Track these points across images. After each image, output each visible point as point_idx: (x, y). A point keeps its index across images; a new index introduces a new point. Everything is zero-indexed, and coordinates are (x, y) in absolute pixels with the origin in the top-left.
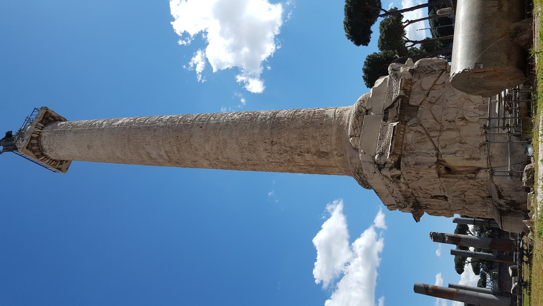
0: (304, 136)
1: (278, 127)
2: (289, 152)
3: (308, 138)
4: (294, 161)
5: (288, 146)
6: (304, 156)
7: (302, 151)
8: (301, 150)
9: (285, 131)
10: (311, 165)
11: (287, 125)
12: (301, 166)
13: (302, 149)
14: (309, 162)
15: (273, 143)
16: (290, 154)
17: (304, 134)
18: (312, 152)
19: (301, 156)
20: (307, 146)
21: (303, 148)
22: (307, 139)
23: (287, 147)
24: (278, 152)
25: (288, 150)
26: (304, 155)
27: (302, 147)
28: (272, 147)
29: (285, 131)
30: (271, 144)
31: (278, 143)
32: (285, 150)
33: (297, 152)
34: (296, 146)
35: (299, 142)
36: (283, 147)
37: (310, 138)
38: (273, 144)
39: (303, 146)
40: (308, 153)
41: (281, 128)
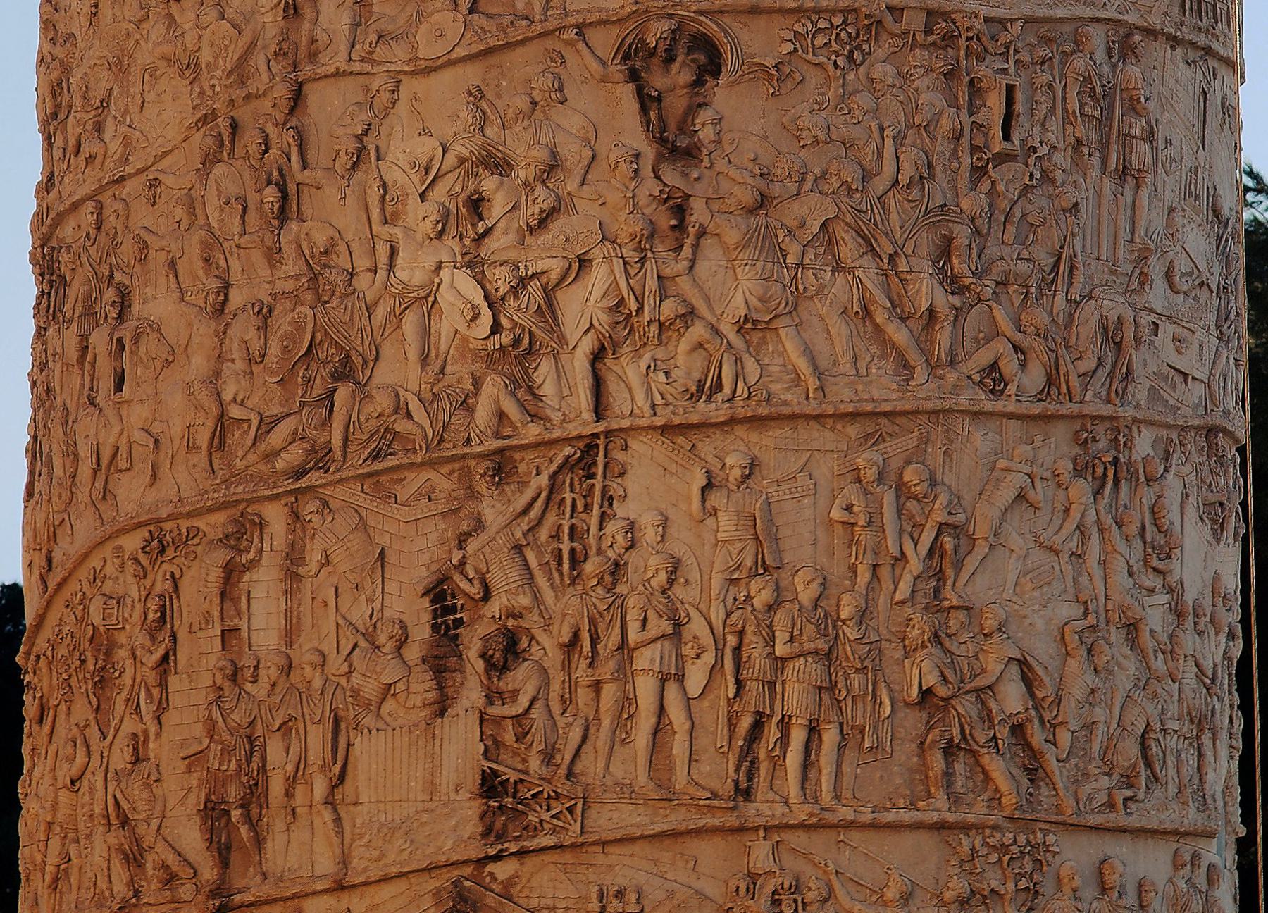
0: (798, 736)
1: (979, 172)
2: (493, 390)
3: (762, 809)
4: (320, 458)
5: (619, 400)
6: (422, 687)
7: (522, 679)
8: (547, 647)
9: (899, 334)
10: (255, 795)
11: (1010, 365)
12: (231, 573)
13: (572, 686)
14: (320, 788)
15: (681, 74)
16: (466, 406)
17: (830, 736)
18: (502, 870)
19: (421, 632)
20: (627, 792)
21: (583, 695)
22: (745, 793)
23: (597, 356)
24: (501, 167)
25: (544, 372)
26: (441, 707)
27: (609, 693)
28: (607, 41)
29: (899, 334)
30: (657, 31)
31: (672, 177)
32: (548, 310)
33: (504, 576)
34: (617, 568)
35: (697, 627)
36: (598, 278)
37: (761, 855)
38: (658, 81)
39: (627, 702)
40: (490, 785)
41: (962, 234)
